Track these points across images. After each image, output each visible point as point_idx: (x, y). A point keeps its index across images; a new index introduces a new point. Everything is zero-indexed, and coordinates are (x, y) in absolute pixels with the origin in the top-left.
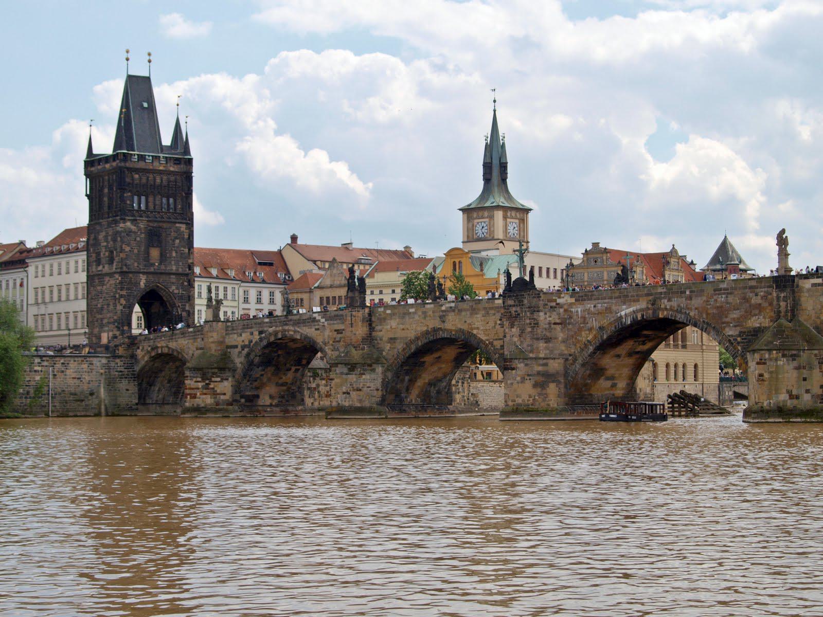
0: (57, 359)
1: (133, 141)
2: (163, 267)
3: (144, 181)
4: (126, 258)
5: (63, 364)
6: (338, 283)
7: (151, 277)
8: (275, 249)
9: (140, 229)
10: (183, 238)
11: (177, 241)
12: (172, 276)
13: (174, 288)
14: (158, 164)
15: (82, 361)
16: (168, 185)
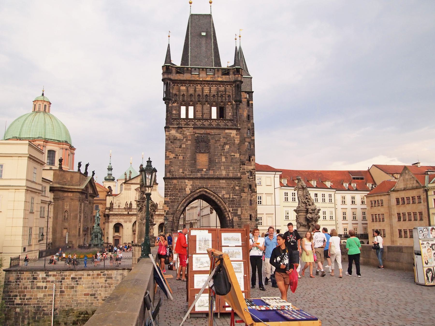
0: (67, 273)
1: (188, 62)
2: (211, 172)
3: (191, 91)
4: (170, 165)
5: (73, 278)
6: (411, 186)
7: (198, 183)
8: (366, 169)
9: (186, 137)
10: (234, 144)
11: (227, 147)
12: (221, 181)
13: (224, 192)
14: (204, 75)
15: (98, 275)
16: (217, 94)
